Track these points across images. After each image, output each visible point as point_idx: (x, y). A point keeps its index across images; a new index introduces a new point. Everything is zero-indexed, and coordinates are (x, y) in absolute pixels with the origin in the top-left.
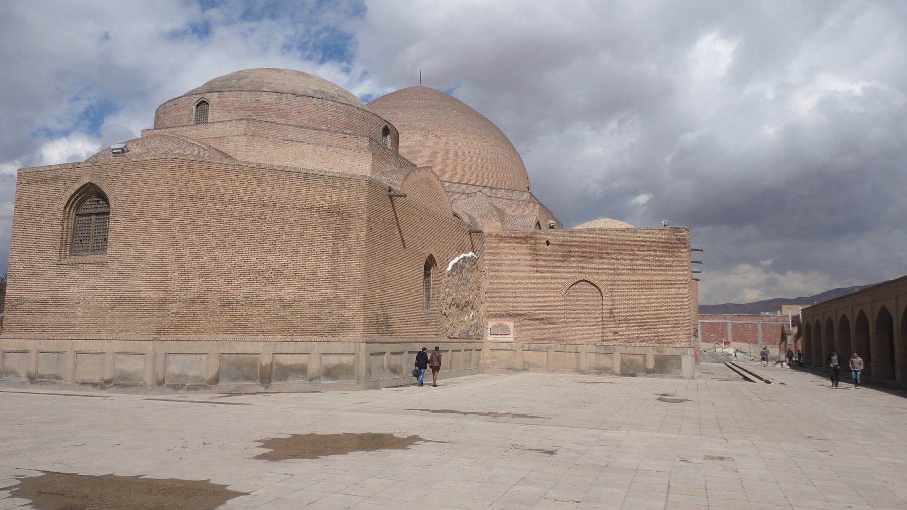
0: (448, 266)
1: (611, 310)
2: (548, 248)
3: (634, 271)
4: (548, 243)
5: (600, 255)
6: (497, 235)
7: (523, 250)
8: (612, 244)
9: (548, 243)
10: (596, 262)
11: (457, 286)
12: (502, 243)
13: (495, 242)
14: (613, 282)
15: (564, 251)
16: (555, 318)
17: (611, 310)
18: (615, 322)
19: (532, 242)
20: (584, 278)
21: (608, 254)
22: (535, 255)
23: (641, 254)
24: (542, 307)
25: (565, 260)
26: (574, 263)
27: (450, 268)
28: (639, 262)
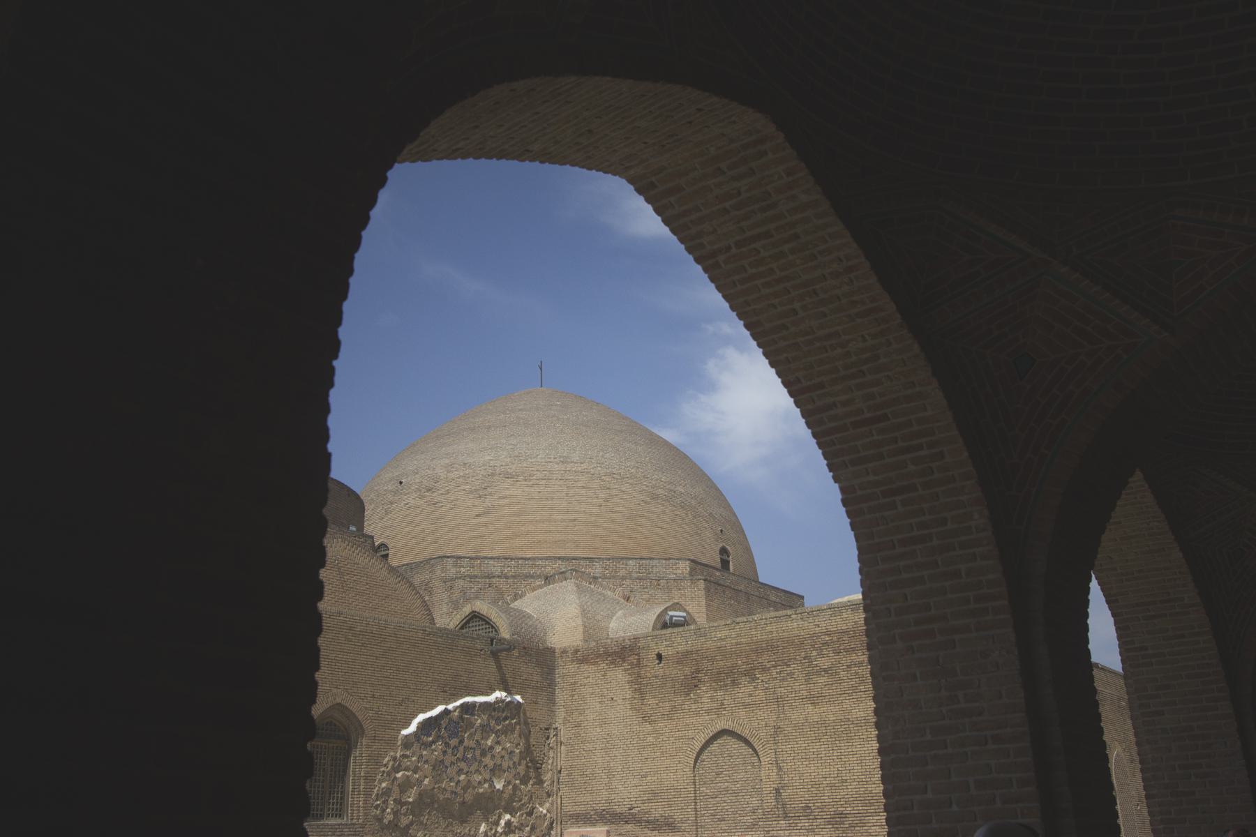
0: (407, 725)
1: (777, 790)
2: (660, 669)
3: (814, 700)
4: (660, 657)
5: (750, 674)
6: (577, 651)
7: (619, 676)
8: (770, 646)
9: (660, 657)
10: (745, 689)
11: (439, 766)
12: (584, 667)
13: (573, 667)
14: (777, 729)
15: (687, 671)
16: (678, 817)
17: (777, 790)
18: (786, 817)
19: (633, 659)
20: (720, 725)
21: (765, 669)
22: (639, 686)
23: (824, 663)
24: (654, 795)
25: (690, 690)
26: (706, 695)
27: (412, 728)
28: (822, 680)
